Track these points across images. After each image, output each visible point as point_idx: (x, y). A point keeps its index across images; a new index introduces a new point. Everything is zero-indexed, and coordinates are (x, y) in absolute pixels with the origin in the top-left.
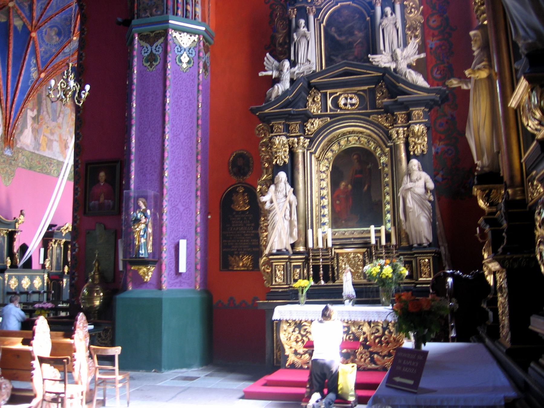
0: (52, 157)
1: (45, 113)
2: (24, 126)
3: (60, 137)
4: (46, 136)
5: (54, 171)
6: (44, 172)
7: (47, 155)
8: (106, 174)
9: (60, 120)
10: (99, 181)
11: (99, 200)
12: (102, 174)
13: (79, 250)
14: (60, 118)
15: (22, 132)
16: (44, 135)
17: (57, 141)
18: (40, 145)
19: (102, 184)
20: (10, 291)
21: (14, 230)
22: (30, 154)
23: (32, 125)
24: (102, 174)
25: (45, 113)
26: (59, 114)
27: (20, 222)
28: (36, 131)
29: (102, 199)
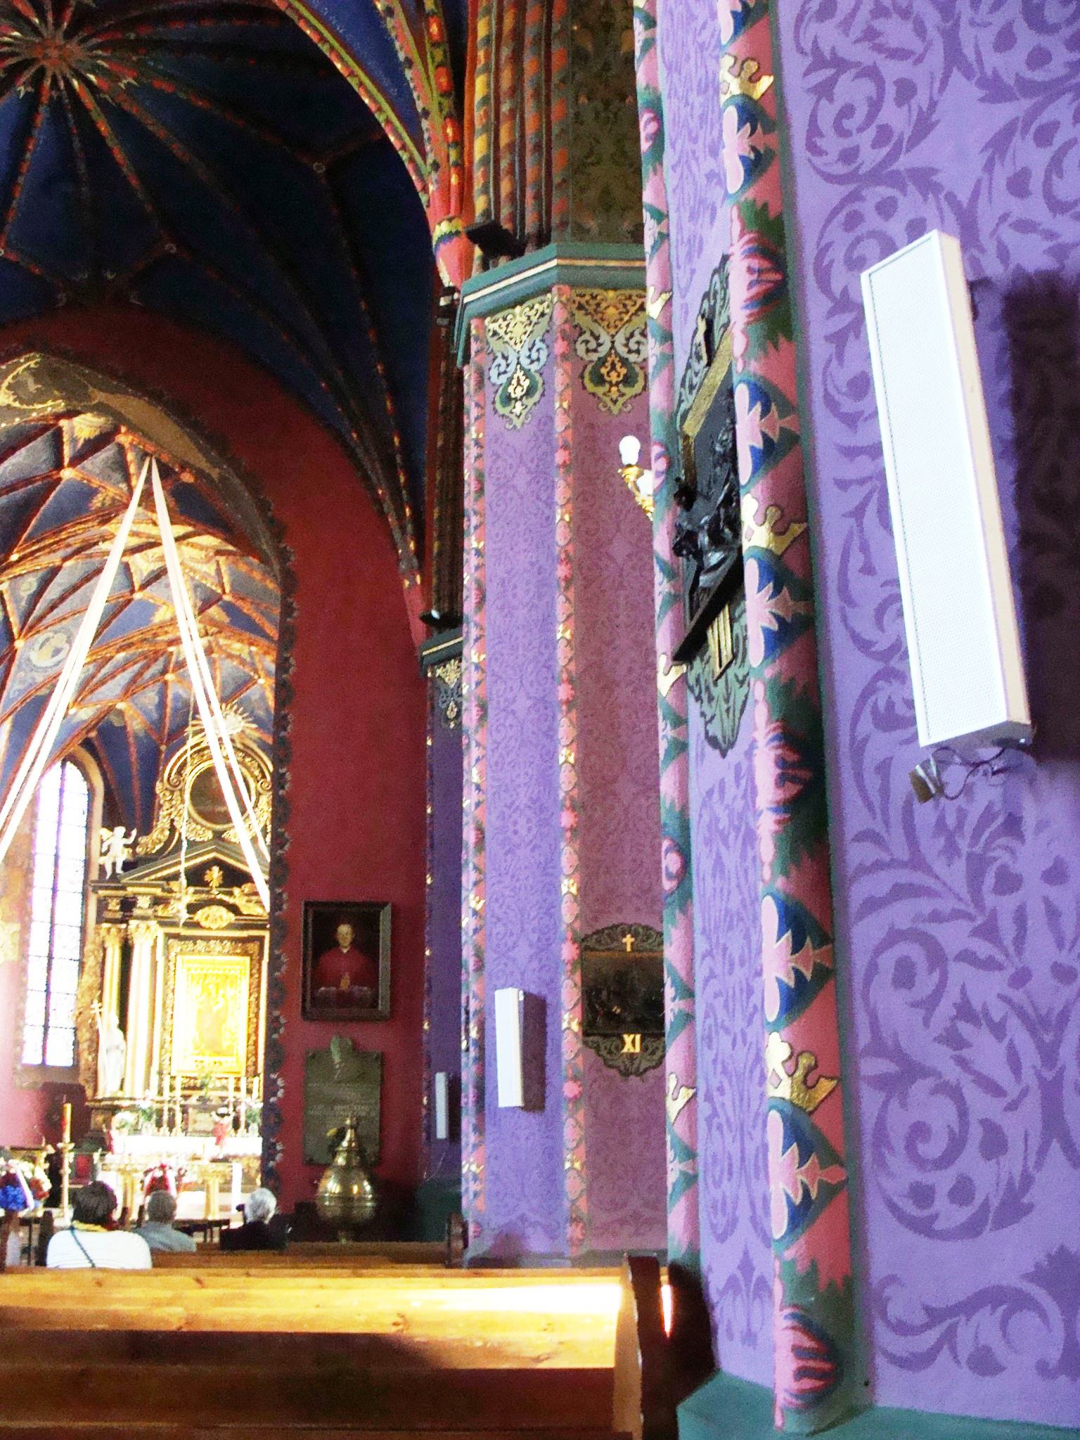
8: (354, 927)
10: (336, 944)
11: (338, 986)
12: (345, 930)
13: (287, 1093)
19: (345, 951)
24: (345, 930)
29: (345, 984)
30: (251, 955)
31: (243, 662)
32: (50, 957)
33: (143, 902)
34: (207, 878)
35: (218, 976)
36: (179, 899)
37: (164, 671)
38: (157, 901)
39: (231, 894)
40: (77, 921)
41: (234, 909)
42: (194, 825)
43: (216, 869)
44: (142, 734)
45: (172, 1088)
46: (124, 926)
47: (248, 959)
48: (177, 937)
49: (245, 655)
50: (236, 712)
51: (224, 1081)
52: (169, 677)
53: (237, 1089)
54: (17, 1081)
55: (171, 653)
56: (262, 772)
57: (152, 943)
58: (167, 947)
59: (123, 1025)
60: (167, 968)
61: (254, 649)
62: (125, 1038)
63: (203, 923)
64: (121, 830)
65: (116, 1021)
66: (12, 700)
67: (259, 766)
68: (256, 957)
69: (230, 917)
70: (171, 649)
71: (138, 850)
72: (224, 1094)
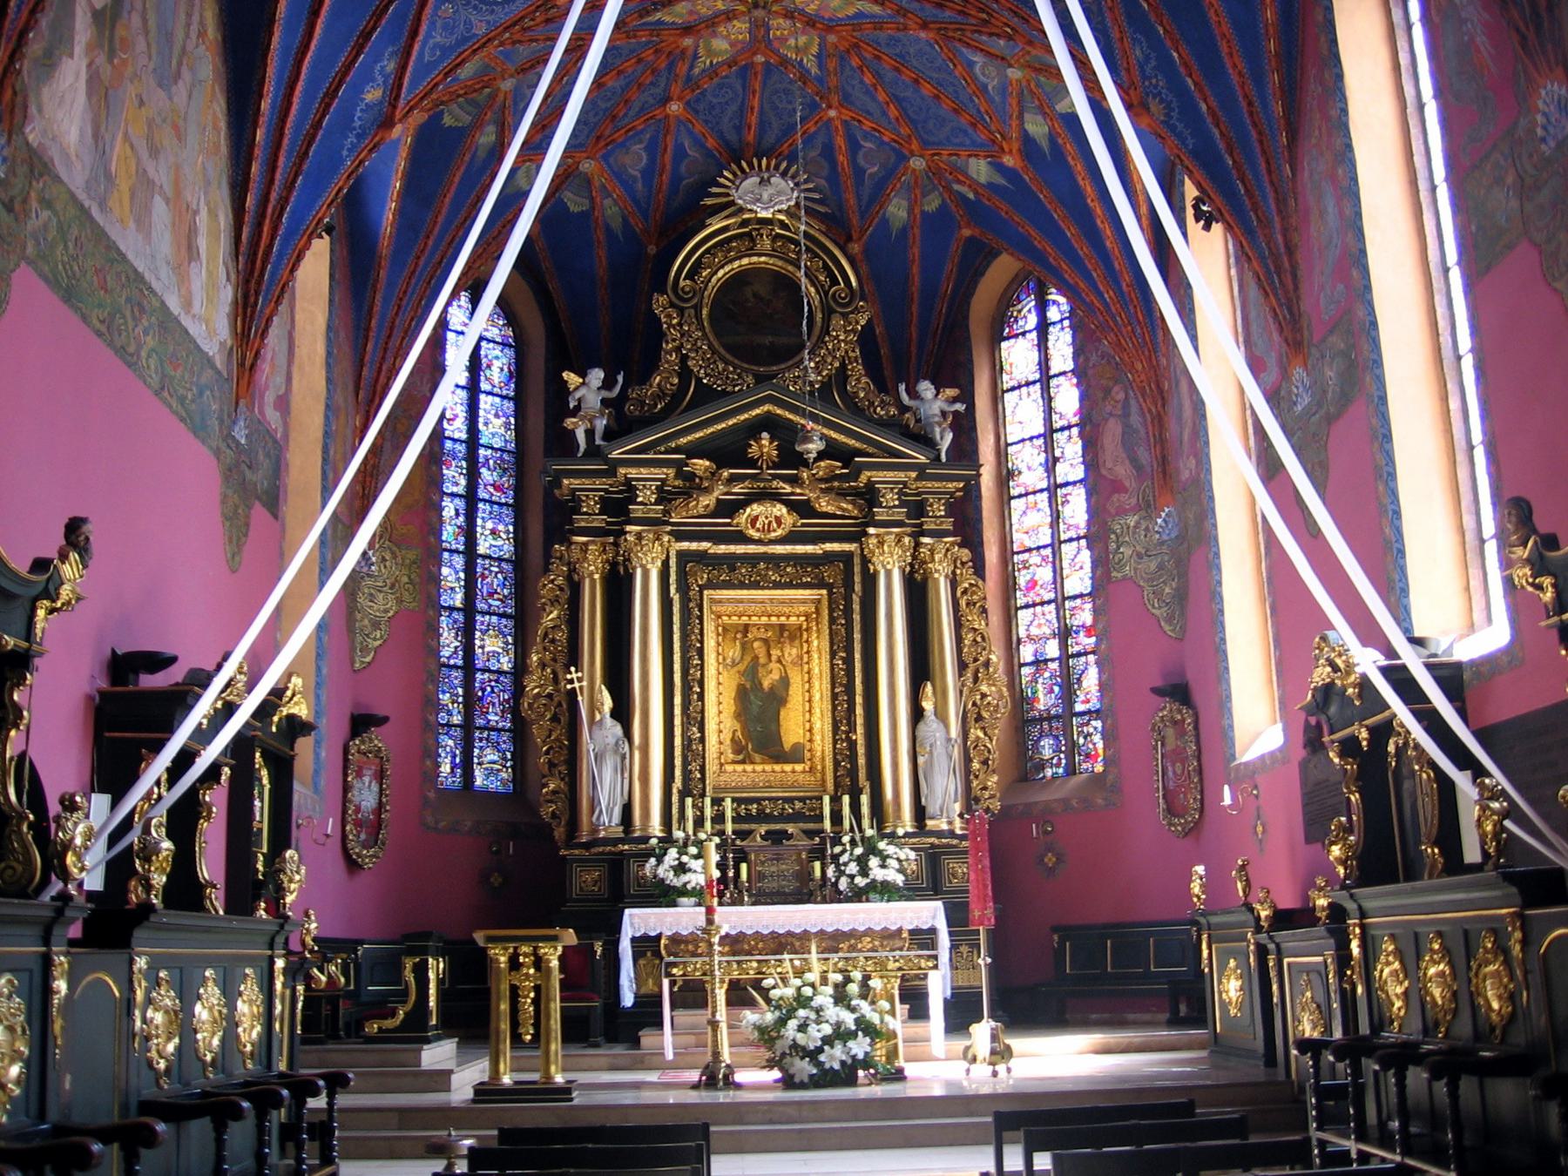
0: (147, 276)
1: (136, 20)
2: (61, 41)
3: (177, 184)
4: (132, 147)
5: (149, 356)
6: (118, 343)
7: (130, 256)
9: (181, 89)
14: (180, 83)
15: (49, 63)
16: (126, 136)
17: (167, 202)
18: (109, 177)
20: (149, 1093)
21: (25, 645)
22: (72, 211)
23: (90, 48)
25: (136, 20)
26: (180, 64)
27: (66, 592)
28: (101, 93)
30: (829, 587)
31: (804, 76)
32: (469, 609)
33: (646, 495)
34: (754, 450)
35: (767, 627)
36: (707, 491)
37: (666, 100)
38: (664, 496)
39: (794, 480)
40: (507, 549)
41: (802, 509)
42: (721, 366)
43: (765, 435)
44: (617, 225)
45: (719, 818)
46: (611, 539)
47: (824, 592)
48: (701, 557)
49: (810, 63)
50: (784, 175)
51: (798, 805)
52: (674, 107)
53: (837, 818)
54: (430, 820)
55: (684, 51)
56: (831, 275)
57: (659, 563)
58: (683, 575)
59: (622, 713)
60: (686, 612)
61: (832, 38)
62: (628, 734)
63: (752, 533)
64: (597, 376)
65: (607, 702)
66: (431, 65)
67: (826, 266)
68: (839, 590)
69: (789, 520)
70: (688, 42)
71: (630, 408)
72: (811, 826)
